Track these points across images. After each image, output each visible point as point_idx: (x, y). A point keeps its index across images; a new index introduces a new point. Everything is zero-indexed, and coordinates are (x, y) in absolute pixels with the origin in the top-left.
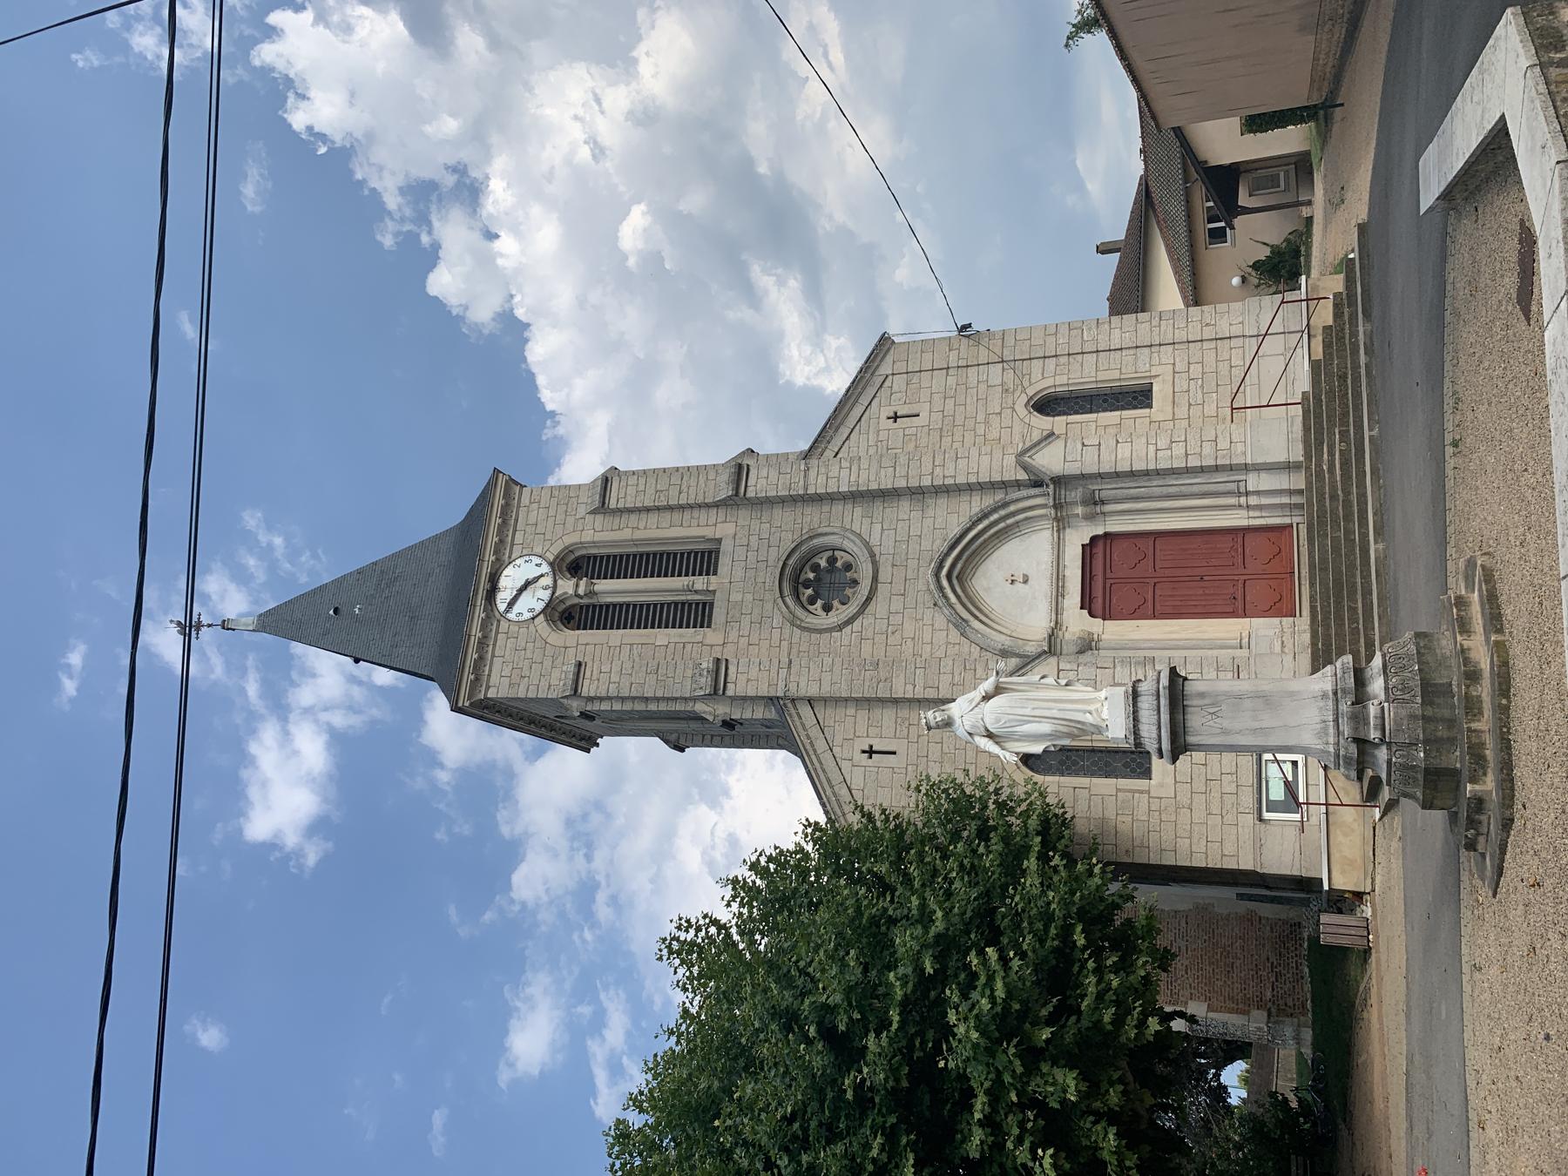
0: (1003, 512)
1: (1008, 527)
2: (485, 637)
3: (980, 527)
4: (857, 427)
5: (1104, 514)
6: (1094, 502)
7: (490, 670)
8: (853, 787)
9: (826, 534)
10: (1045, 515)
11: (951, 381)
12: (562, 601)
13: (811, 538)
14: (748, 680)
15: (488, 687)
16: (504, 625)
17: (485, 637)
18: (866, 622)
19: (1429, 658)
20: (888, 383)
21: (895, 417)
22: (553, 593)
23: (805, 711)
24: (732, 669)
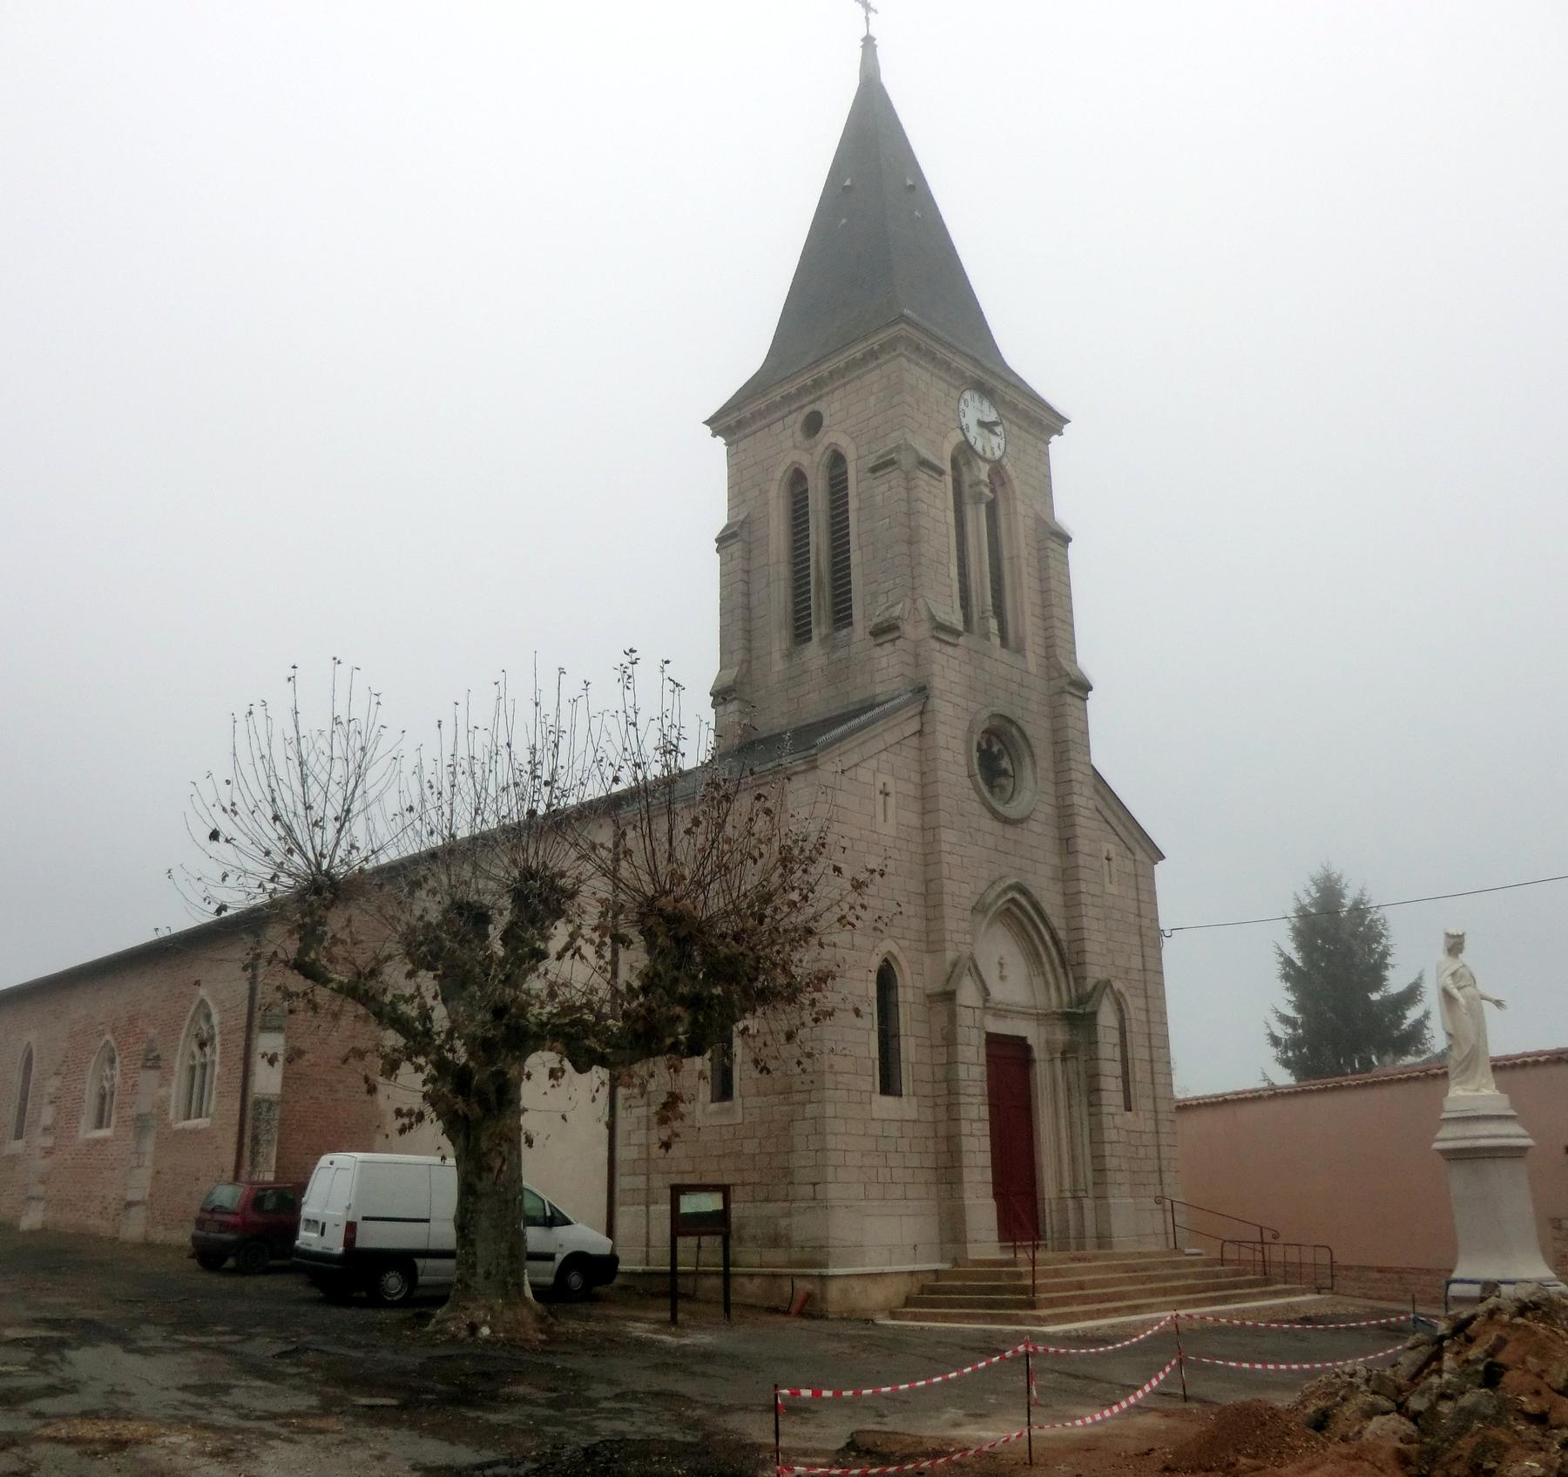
0: (1057, 961)
1: (1041, 963)
2: (949, 368)
3: (1047, 937)
4: (1101, 819)
5: (1052, 1060)
6: (1067, 1053)
7: (921, 367)
8: (858, 769)
9: (1034, 773)
10: (1050, 1000)
11: (1132, 918)
12: (968, 463)
13: (1032, 755)
14: (943, 667)
15: (909, 360)
16: (955, 393)
17: (949, 368)
18: (975, 804)
19: (423, 1410)
20: (1130, 856)
21: (1108, 859)
22: (980, 457)
23: (914, 726)
24: (950, 650)
